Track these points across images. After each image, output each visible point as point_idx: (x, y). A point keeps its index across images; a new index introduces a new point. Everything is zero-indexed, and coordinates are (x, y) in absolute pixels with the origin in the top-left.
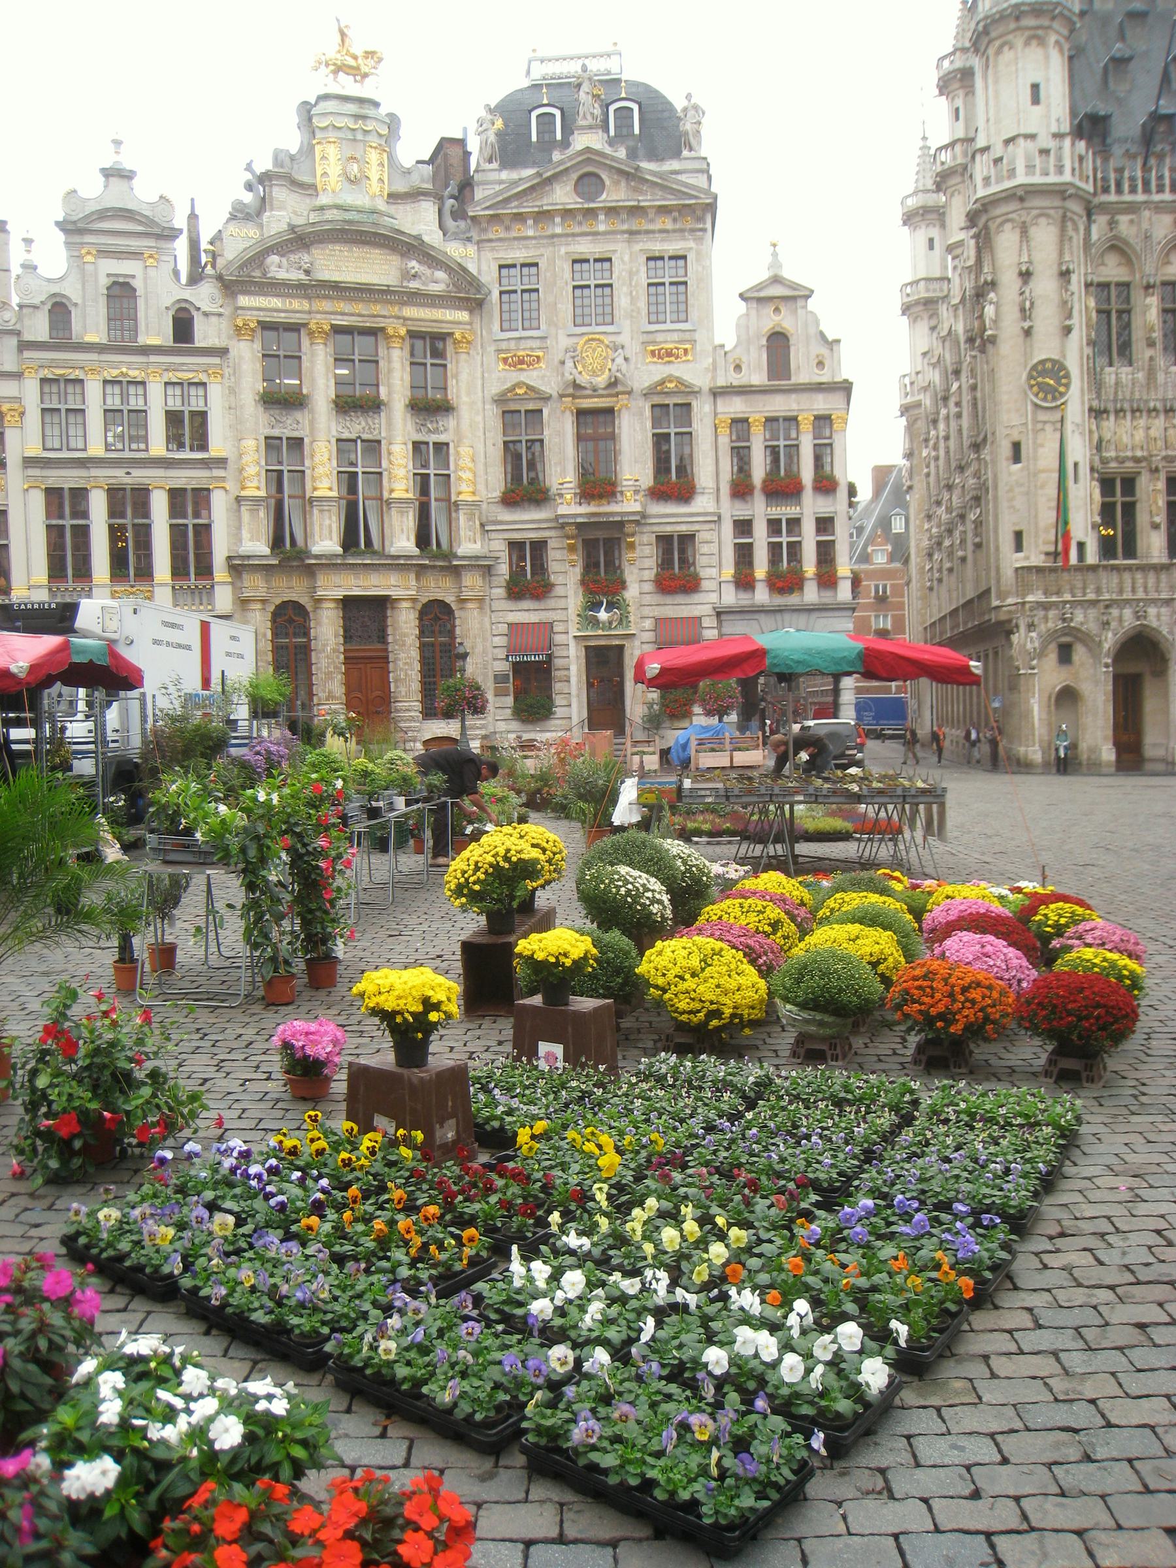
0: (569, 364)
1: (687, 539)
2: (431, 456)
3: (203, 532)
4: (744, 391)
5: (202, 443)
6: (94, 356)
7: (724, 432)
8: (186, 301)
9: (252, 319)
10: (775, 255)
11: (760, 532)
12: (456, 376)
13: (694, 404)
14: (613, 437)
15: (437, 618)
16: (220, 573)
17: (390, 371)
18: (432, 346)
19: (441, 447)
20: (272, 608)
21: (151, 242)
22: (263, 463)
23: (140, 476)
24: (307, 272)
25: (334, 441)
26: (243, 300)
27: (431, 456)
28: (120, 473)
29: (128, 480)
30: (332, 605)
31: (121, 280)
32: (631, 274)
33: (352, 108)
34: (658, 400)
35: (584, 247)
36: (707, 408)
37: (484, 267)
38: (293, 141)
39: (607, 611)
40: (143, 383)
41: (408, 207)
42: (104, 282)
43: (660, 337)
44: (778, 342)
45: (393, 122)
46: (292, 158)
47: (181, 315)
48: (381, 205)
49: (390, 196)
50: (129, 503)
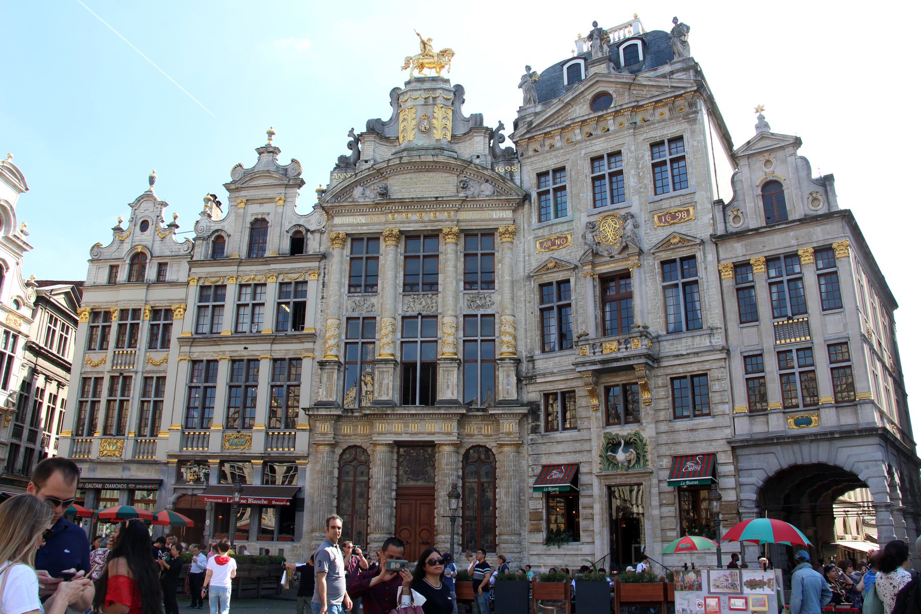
0: (589, 236)
2: (479, 325)
4: (740, 235)
7: (728, 275)
8: (300, 225)
9: (342, 231)
10: (761, 118)
11: (771, 364)
12: (500, 261)
13: (699, 255)
14: (630, 296)
16: (302, 421)
17: (446, 260)
20: (339, 451)
21: (282, 190)
22: (343, 337)
24: (382, 195)
25: (399, 318)
26: (337, 220)
27: (479, 325)
28: (241, 347)
29: (245, 353)
30: (385, 449)
31: (260, 217)
32: (637, 159)
33: (427, 85)
34: (665, 256)
35: (601, 146)
36: (711, 257)
37: (526, 178)
38: (385, 113)
39: (624, 451)
40: (265, 285)
41: (467, 144)
42: (250, 219)
43: (665, 204)
44: (772, 190)
45: (459, 91)
46: (384, 124)
47: (299, 236)
49: (453, 136)
50: (244, 369)
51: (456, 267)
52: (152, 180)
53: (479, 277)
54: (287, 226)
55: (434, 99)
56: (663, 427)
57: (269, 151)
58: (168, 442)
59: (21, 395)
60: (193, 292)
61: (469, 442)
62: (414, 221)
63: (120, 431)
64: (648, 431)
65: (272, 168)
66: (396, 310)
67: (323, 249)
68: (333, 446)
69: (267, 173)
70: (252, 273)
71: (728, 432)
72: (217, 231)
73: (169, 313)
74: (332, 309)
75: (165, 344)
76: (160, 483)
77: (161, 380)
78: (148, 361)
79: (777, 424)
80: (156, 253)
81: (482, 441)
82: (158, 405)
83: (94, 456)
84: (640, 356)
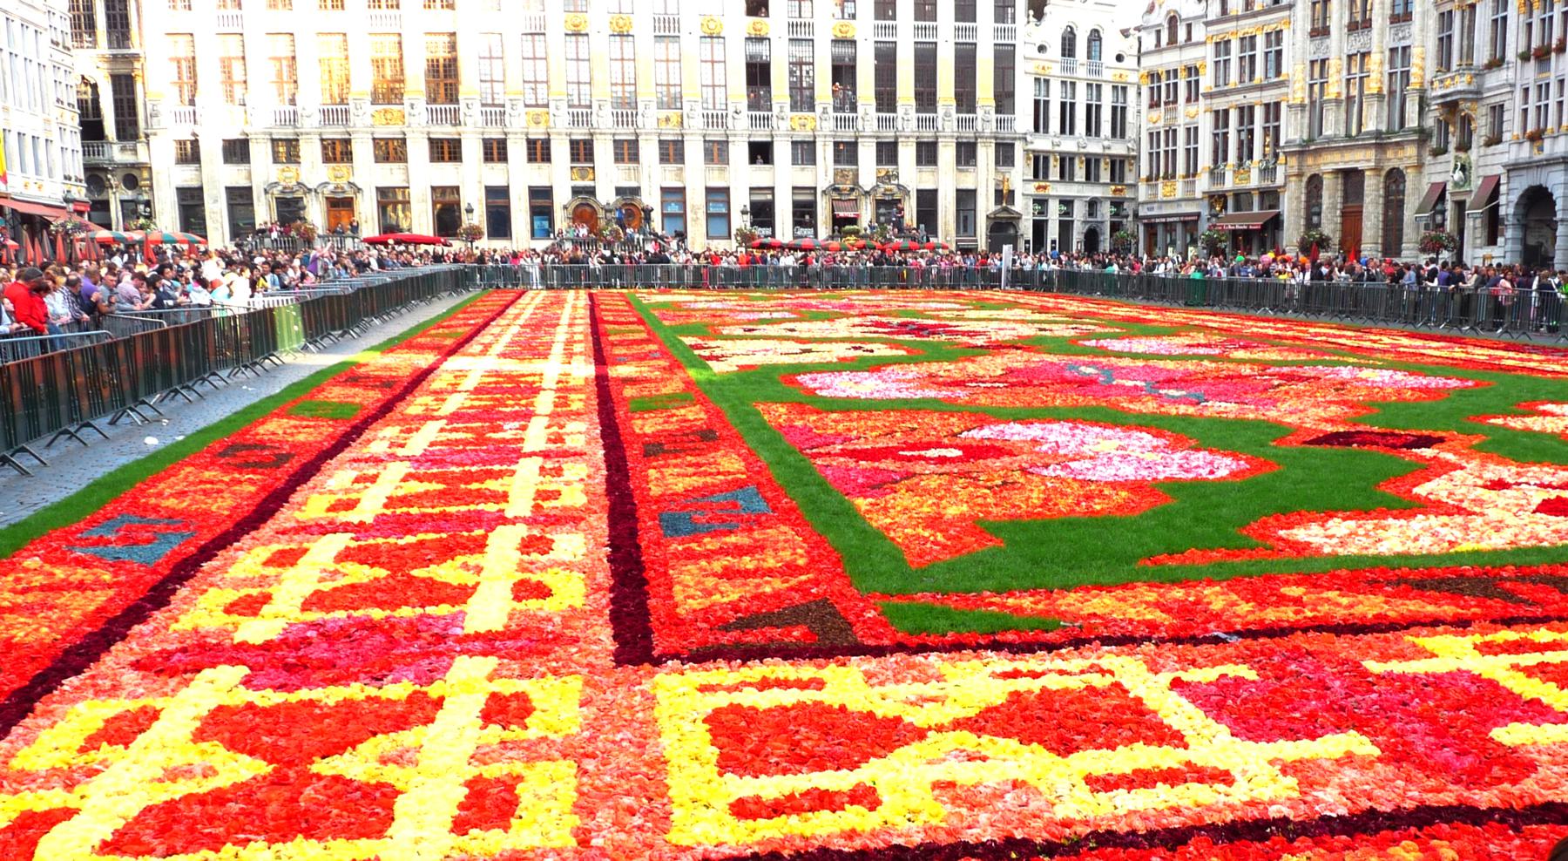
5: (1278, 73)
11: (1533, 94)
15: (1394, 179)
20: (1305, 179)
50: (1246, 113)
60: (1209, 50)
61: (1388, 166)
63: (1174, 177)
66: (1341, 50)
68: (1300, 175)
70: (1247, 27)
71: (1505, 159)
73: (1197, 73)
74: (1298, 56)
75: (1197, 99)
76: (1199, 215)
77: (1196, 129)
79: (1525, 152)
81: (1394, 164)
82: (1196, 150)
83: (1160, 197)
84: (1460, 92)
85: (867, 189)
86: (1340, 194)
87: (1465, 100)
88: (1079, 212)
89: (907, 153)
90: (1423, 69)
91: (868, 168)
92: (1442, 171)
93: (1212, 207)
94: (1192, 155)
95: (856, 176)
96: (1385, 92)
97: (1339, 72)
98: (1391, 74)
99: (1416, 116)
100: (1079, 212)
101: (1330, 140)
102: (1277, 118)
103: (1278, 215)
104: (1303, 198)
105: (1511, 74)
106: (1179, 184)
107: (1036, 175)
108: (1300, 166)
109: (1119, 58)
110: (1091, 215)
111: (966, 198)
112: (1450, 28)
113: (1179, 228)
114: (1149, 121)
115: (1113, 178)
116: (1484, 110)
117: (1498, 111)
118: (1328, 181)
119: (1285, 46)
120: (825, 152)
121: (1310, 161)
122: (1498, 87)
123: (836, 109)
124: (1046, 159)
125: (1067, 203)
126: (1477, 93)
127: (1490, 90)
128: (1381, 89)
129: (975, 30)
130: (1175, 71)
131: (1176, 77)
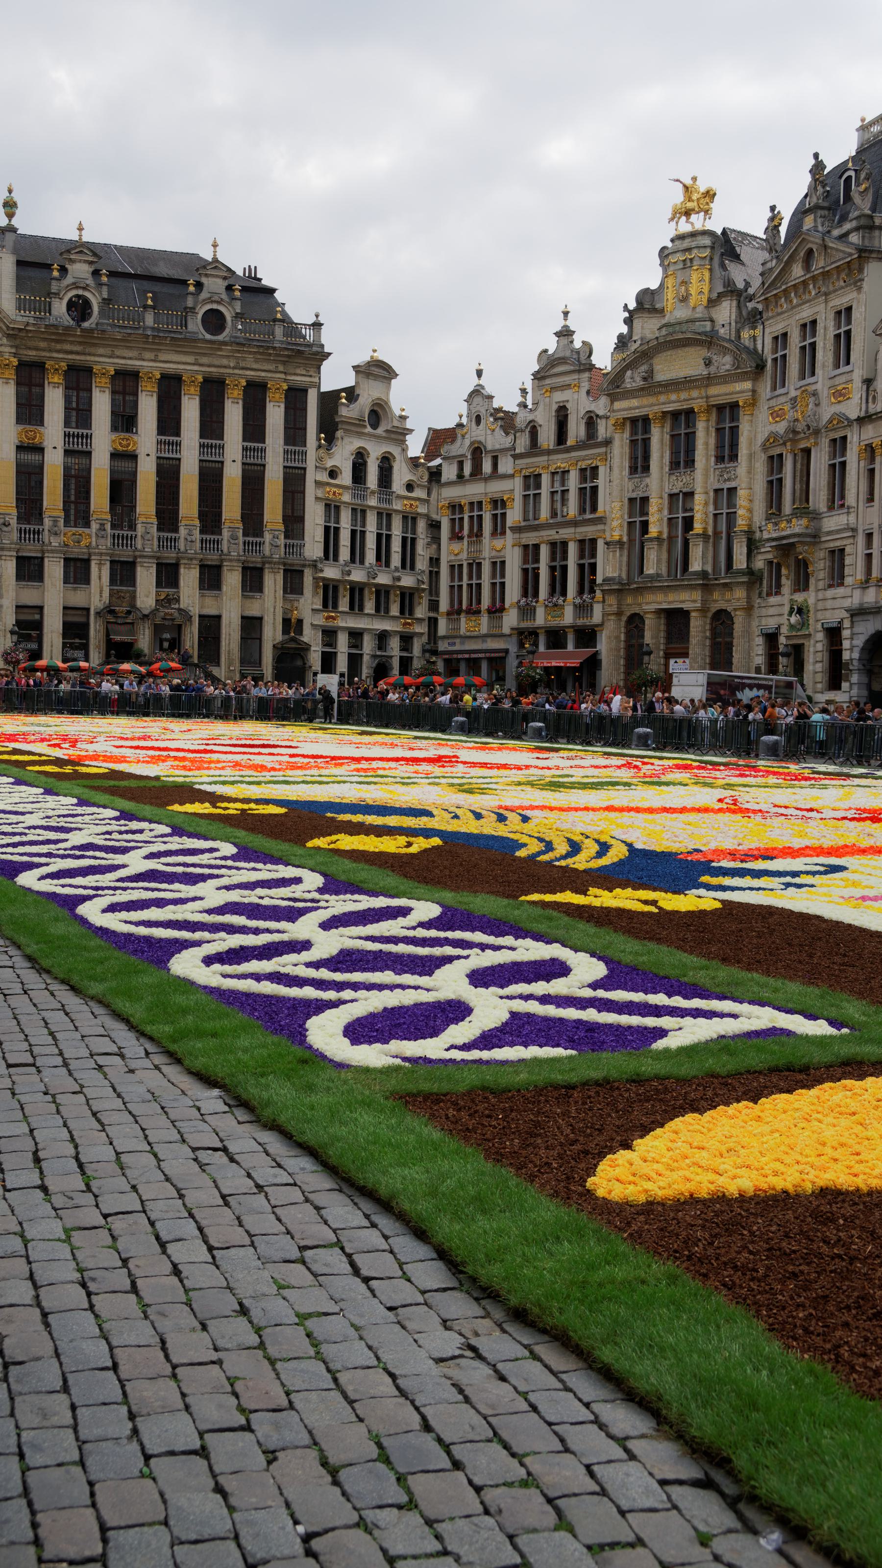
1: (842, 551)
3: (593, 566)
5: (594, 509)
6: (545, 458)
15: (722, 621)
18: (728, 412)
19: (732, 491)
20: (624, 618)
21: (576, 376)
23: (565, 533)
24: (645, 379)
25: (666, 496)
26: (618, 405)
28: (553, 532)
29: (557, 537)
36: (855, 439)
42: (555, 407)
48: (700, 313)
49: (710, 301)
50: (559, 549)
51: (707, 444)
52: (479, 373)
53: (727, 451)
54: (582, 412)
55: (691, 260)
56: (821, 595)
57: (565, 334)
58: (511, 620)
59: (431, 572)
60: (518, 482)
61: (715, 607)
62: (673, 402)
64: (811, 601)
65: (568, 354)
66: (662, 489)
67: (608, 435)
68: (619, 614)
69: (562, 360)
70: (560, 461)
71: (847, 603)
72: (530, 422)
74: (616, 493)
75: (503, 533)
76: (507, 651)
77: (503, 563)
78: (493, 549)
80: (489, 448)
81: (721, 605)
82: (503, 585)
83: (463, 631)
85: (146, 612)
86: (662, 634)
87: (803, 543)
88: (368, 646)
89: (189, 578)
90: (750, 511)
91: (146, 591)
92: (775, 612)
93: (521, 645)
94: (499, 589)
95: (133, 597)
96: (710, 533)
97: (660, 510)
98: (715, 515)
99: (744, 558)
100: (368, 646)
101: (650, 576)
102: (593, 555)
103: (596, 654)
104: (623, 637)
105: (852, 519)
106: (484, 619)
107: (325, 605)
108: (619, 605)
109: (410, 487)
110: (380, 648)
111: (251, 626)
112: (780, 470)
113: (484, 666)
114: (450, 553)
115: (402, 612)
116: (822, 554)
117: (838, 555)
118: (649, 622)
119: (601, 482)
120: (100, 574)
121: (629, 600)
122: (838, 531)
123: (113, 527)
124: (336, 589)
125: (356, 636)
126: (815, 536)
127: (829, 533)
128: (705, 529)
129: (263, 450)
130: (480, 503)
131: (480, 509)
